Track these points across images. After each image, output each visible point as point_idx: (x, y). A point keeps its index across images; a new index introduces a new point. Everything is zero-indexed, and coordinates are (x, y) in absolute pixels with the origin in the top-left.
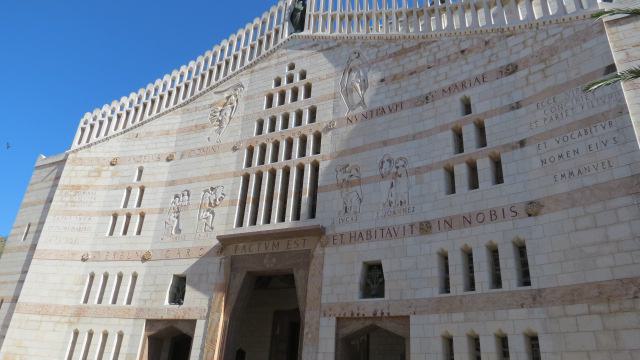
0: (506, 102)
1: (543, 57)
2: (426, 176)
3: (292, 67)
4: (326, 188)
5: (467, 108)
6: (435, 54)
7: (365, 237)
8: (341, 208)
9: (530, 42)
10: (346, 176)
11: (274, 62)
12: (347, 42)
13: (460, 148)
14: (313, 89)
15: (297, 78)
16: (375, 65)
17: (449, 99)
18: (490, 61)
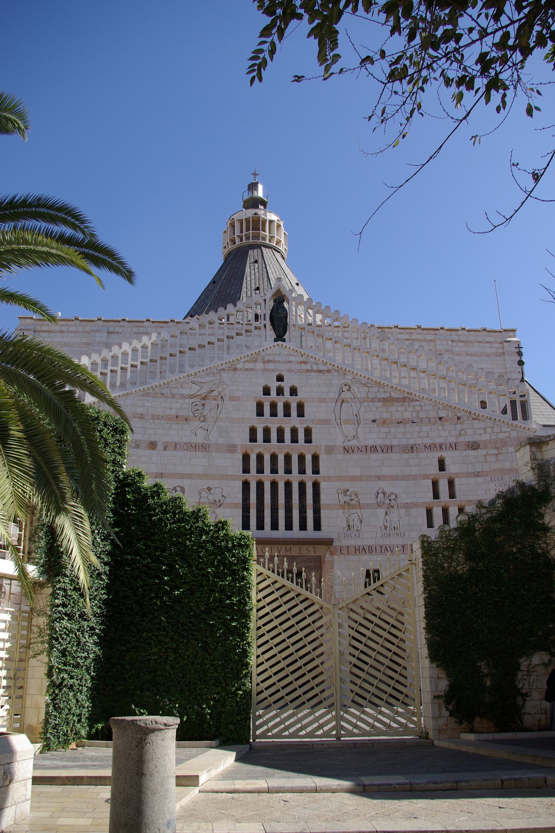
0: (471, 470)
1: (497, 446)
2: (413, 511)
3: (280, 378)
4: (329, 507)
5: (442, 466)
6: (418, 412)
7: (367, 551)
8: (345, 525)
9: (489, 430)
10: (347, 499)
11: (260, 366)
12: (338, 371)
13: (436, 495)
14: (306, 410)
15: (287, 392)
16: (366, 404)
17: (430, 455)
18: (460, 434)
